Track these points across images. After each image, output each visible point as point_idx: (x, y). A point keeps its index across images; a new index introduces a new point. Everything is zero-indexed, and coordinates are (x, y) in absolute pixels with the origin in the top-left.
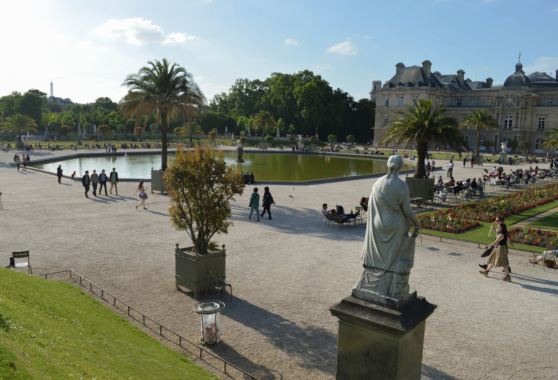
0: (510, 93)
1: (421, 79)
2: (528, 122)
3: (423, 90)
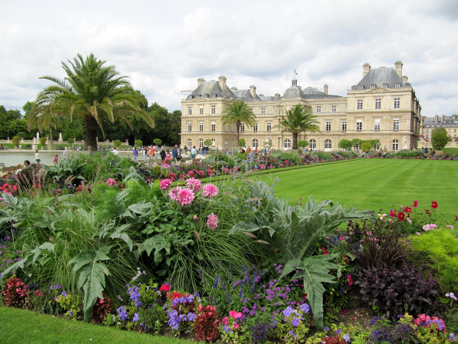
1: (217, 92)
3: (219, 100)
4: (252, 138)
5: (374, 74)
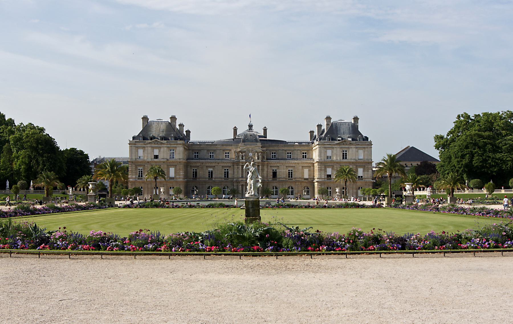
0: (251, 149)
2: (265, 172)
3: (180, 144)
4: (207, 186)
5: (336, 127)
